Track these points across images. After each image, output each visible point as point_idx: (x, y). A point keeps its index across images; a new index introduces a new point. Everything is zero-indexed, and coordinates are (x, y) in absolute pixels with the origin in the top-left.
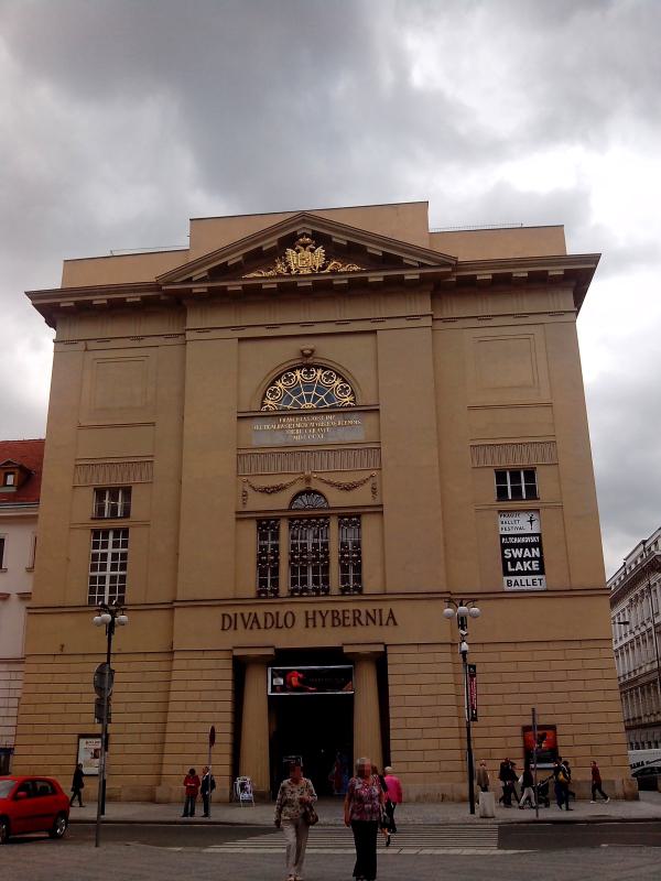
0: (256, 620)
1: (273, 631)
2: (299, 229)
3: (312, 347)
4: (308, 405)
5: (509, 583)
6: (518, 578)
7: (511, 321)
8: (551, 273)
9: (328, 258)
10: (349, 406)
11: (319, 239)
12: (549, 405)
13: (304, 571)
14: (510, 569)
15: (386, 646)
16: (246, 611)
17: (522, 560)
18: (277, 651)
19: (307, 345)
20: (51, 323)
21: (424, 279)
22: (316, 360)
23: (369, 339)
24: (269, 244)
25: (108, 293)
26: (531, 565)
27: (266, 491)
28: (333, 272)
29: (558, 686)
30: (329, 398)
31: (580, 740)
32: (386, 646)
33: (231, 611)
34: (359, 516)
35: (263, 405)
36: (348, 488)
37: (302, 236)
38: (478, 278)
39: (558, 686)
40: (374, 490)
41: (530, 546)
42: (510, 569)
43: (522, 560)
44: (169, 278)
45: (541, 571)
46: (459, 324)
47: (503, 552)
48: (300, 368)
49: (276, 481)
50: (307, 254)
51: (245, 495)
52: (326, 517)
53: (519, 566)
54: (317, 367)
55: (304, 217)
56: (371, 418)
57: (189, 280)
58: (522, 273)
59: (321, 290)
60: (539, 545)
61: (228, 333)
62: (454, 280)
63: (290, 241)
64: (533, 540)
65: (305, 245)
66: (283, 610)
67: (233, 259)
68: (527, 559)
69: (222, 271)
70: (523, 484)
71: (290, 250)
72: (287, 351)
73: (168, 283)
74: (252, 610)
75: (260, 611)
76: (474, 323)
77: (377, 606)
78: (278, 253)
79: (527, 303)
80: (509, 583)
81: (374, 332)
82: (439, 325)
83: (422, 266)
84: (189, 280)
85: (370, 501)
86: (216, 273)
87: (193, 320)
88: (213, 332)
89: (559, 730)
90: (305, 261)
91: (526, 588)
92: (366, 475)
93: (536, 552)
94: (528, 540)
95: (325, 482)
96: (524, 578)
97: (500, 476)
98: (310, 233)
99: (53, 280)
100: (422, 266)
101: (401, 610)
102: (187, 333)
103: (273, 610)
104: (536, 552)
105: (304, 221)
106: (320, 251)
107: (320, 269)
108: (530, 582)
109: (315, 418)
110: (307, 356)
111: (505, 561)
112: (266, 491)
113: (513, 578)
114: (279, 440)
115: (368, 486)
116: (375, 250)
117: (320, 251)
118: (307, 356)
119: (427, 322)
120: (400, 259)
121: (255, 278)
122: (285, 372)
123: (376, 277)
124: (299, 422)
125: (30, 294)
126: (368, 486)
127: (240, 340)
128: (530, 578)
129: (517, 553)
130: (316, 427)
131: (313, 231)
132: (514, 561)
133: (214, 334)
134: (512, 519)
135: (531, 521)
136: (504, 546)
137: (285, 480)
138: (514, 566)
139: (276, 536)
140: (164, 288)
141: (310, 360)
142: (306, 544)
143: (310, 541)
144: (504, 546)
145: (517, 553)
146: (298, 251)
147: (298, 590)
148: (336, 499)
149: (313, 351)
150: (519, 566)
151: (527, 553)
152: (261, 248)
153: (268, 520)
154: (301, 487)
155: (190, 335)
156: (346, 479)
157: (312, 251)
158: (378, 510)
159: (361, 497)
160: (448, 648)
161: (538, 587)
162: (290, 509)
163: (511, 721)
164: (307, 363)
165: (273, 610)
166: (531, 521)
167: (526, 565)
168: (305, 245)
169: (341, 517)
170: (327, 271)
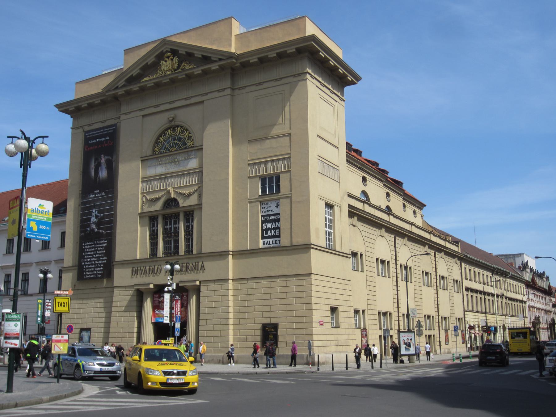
2: (164, 49)
3: (172, 116)
5: (264, 243)
6: (268, 240)
7: (273, 84)
8: (288, 52)
10: (192, 147)
12: (289, 135)
13: (170, 241)
14: (265, 235)
19: (171, 114)
20: (71, 117)
21: (222, 68)
22: (176, 123)
23: (200, 107)
24: (151, 60)
25: (87, 100)
26: (275, 232)
29: (282, 301)
30: (185, 144)
32: (200, 282)
34: (193, 211)
36: (189, 195)
38: (251, 62)
42: (265, 235)
43: (271, 229)
44: (107, 89)
46: (247, 89)
47: (262, 227)
48: (170, 128)
50: (169, 62)
52: (179, 213)
53: (269, 233)
54: (178, 127)
55: (164, 42)
57: (117, 88)
58: (273, 54)
59: (173, 84)
60: (279, 220)
62: (238, 64)
63: (161, 57)
64: (277, 217)
65: (168, 57)
67: (135, 72)
68: (274, 229)
69: (132, 80)
70: (274, 184)
71: (163, 63)
73: (108, 91)
76: (254, 88)
79: (280, 72)
81: (202, 102)
82: (237, 92)
83: (220, 60)
84: (117, 88)
87: (124, 109)
88: (132, 113)
89: (280, 326)
91: (272, 245)
96: (271, 240)
97: (263, 180)
98: (169, 50)
99: (70, 96)
100: (220, 60)
102: (121, 116)
105: (165, 44)
106: (176, 59)
107: (175, 70)
108: (274, 242)
109: (175, 157)
110: (171, 121)
111: (263, 230)
113: (266, 240)
114: (160, 170)
116: (198, 55)
117: (176, 59)
118: (171, 121)
119: (228, 92)
120: (210, 57)
121: (146, 81)
122: (163, 133)
123: (198, 71)
125: (57, 106)
127: (144, 116)
129: (269, 226)
130: (175, 162)
131: (171, 49)
132: (267, 230)
133: (132, 115)
134: (268, 206)
135: (277, 206)
138: (267, 234)
140: (107, 94)
141: (173, 123)
142: (171, 228)
143: (173, 226)
144: (263, 222)
145: (269, 226)
146: (166, 61)
147: (167, 253)
149: (173, 118)
150: (269, 233)
152: (147, 63)
155: (123, 117)
156: (186, 191)
157: (172, 60)
166: (277, 206)
168: (168, 57)
170: (180, 70)
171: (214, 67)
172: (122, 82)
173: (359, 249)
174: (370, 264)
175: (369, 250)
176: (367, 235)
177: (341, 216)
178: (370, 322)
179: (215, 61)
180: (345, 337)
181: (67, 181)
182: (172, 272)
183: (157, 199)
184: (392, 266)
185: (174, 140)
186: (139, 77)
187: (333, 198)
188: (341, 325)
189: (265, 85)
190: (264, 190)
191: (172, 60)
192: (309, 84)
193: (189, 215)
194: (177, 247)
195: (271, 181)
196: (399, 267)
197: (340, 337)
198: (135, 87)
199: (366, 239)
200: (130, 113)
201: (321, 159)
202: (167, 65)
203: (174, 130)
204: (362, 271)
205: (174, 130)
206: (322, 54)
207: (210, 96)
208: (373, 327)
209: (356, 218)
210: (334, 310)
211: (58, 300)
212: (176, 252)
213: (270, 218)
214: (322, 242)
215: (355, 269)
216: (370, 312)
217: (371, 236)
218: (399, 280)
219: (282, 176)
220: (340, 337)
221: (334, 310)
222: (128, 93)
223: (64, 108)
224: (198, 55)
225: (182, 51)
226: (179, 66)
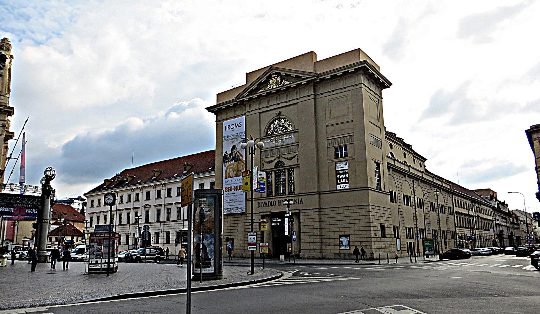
0: (266, 204)
1: (270, 207)
4: (279, 132)
9: (282, 80)
11: (278, 74)
15: (300, 210)
16: (264, 201)
17: (342, 179)
18: (272, 213)
19: (278, 111)
23: (295, 106)
27: (268, 163)
28: (284, 85)
30: (286, 129)
31: (357, 240)
33: (260, 202)
35: (267, 133)
37: (273, 74)
39: (351, 222)
40: (298, 159)
41: (345, 173)
43: (342, 179)
45: (348, 183)
46: (324, 95)
49: (270, 159)
51: (263, 164)
53: (341, 181)
55: (271, 68)
56: (296, 134)
61: (257, 111)
63: (270, 77)
64: (346, 171)
65: (274, 77)
66: (273, 200)
68: (344, 178)
72: (273, 114)
74: (265, 201)
75: (267, 201)
77: (298, 198)
78: (267, 82)
80: (338, 187)
81: (297, 103)
83: (307, 78)
84: (244, 97)
85: (297, 163)
86: (251, 93)
90: (274, 83)
92: (295, 154)
93: (347, 176)
94: (345, 171)
95: (285, 158)
97: (336, 149)
99: (214, 103)
100: (307, 78)
101: (304, 198)
103: (270, 201)
104: (347, 176)
105: (272, 70)
106: (279, 78)
110: (277, 115)
111: (337, 179)
112: (268, 163)
113: (339, 185)
114: (272, 145)
115: (296, 158)
116: (293, 75)
123: (293, 85)
124: (277, 138)
125: (206, 108)
126: (296, 158)
127: (260, 113)
128: (345, 185)
129: (341, 176)
132: (340, 179)
133: (253, 112)
136: (337, 174)
137: (273, 159)
139: (272, 177)
144: (337, 174)
145: (341, 176)
148: (287, 163)
149: (280, 113)
150: (341, 181)
151: (344, 176)
153: (269, 172)
154: (277, 160)
158: (298, 166)
159: (294, 162)
160: (317, 210)
161: (347, 188)
162: (275, 168)
163: (336, 233)
164: (279, 117)
165: (270, 201)
167: (344, 180)
168: (274, 77)
169: (288, 170)
171: (304, 82)
172: (246, 93)
173: (394, 190)
174: (400, 199)
175: (399, 189)
176: (398, 180)
177: (384, 169)
178: (401, 234)
179: (304, 79)
180: (389, 243)
181: (214, 152)
182: (288, 205)
183: (272, 161)
184: (412, 199)
185: (280, 126)
186: (257, 89)
187: (379, 159)
188: (387, 236)
189: (335, 92)
190: (337, 155)
191: (276, 79)
192: (364, 90)
193: (291, 170)
194: (284, 190)
195: (341, 150)
196: (416, 200)
197: (386, 243)
198: (255, 96)
199: (397, 183)
200: (251, 111)
201: (371, 135)
202: (274, 83)
203: (279, 121)
204: (396, 202)
205: (279, 121)
206: (371, 71)
207: (301, 100)
208: (403, 237)
209: (391, 170)
210: (383, 227)
211: (262, 224)
212: (284, 194)
213: (341, 172)
214: (375, 186)
215: (392, 201)
216: (401, 228)
217: (400, 181)
218: (417, 207)
219: (348, 147)
220: (386, 243)
221: (383, 227)
222: (250, 99)
223: (209, 109)
224: (293, 75)
225: (283, 74)
226: (281, 83)
